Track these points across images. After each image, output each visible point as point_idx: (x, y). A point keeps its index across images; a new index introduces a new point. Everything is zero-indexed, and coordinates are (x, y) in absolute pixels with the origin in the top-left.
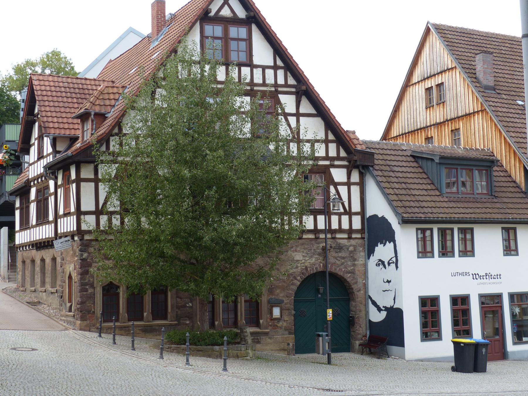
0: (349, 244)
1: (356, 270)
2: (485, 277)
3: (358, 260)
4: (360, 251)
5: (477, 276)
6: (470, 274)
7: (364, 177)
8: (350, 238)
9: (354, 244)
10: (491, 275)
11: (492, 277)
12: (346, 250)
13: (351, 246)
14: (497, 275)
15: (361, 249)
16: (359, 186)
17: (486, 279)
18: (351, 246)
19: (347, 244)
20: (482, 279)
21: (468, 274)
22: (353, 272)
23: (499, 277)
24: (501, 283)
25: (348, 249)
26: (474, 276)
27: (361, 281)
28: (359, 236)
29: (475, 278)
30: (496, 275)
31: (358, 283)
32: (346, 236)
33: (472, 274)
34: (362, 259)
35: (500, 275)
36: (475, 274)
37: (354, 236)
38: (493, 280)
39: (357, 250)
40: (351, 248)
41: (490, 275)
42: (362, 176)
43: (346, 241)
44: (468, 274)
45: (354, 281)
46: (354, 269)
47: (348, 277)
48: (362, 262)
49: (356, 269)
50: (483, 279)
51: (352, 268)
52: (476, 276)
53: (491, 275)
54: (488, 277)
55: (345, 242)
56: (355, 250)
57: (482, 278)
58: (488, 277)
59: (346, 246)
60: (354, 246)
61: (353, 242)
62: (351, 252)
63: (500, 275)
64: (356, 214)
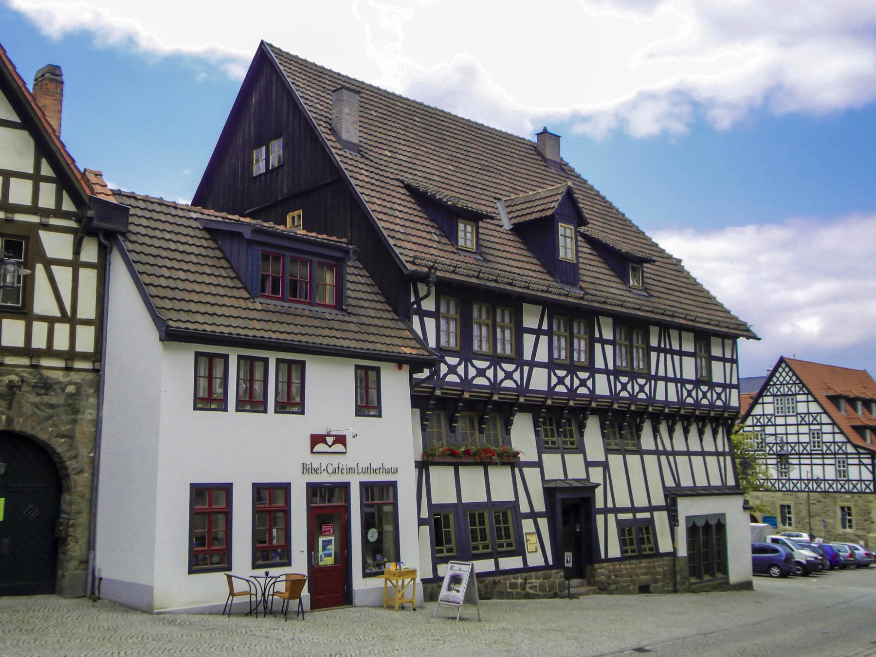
0: (68, 379)
1: (76, 432)
3: (83, 413)
4: (88, 396)
7: (108, 254)
8: (68, 369)
9: (79, 381)
12: (59, 391)
13: (70, 383)
15: (92, 391)
16: (95, 271)
18: (70, 383)
19: (62, 379)
22: (70, 436)
25: (63, 390)
27: (86, 454)
28: (88, 365)
31: (80, 457)
32: (61, 364)
34: (90, 411)
37: (78, 365)
39: (83, 393)
40: (71, 389)
42: (104, 252)
43: (61, 373)
45: (73, 453)
46: (73, 430)
47: (59, 446)
48: (90, 417)
49: (78, 429)
51: (70, 426)
55: (59, 375)
56: (78, 392)
59: (60, 383)
60: (76, 384)
61: (75, 377)
62: (70, 396)
64: (86, 322)
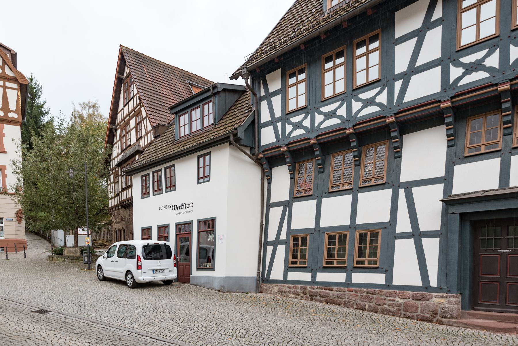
2: (181, 208)
5: (176, 207)
6: (171, 206)
10: (186, 205)
11: (186, 207)
14: (190, 204)
17: (182, 209)
20: (179, 210)
21: (170, 207)
23: (191, 205)
24: (193, 211)
26: (174, 207)
29: (174, 209)
30: (189, 204)
33: (172, 206)
35: (192, 204)
36: (174, 206)
38: (187, 209)
41: (185, 205)
44: (170, 207)
50: (180, 209)
52: (175, 207)
53: (186, 205)
54: (183, 207)
57: (179, 208)
58: (183, 207)
63: (192, 204)
